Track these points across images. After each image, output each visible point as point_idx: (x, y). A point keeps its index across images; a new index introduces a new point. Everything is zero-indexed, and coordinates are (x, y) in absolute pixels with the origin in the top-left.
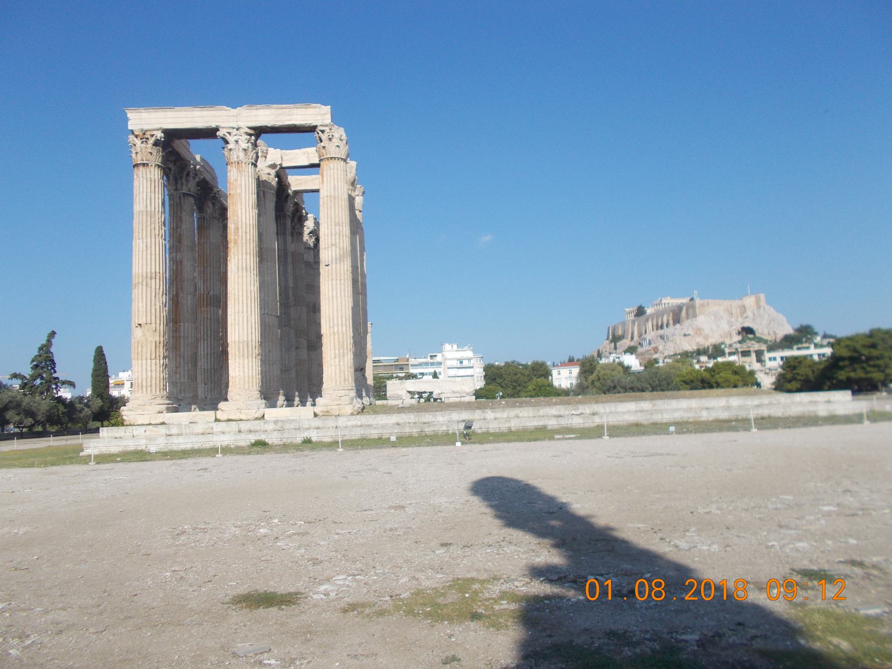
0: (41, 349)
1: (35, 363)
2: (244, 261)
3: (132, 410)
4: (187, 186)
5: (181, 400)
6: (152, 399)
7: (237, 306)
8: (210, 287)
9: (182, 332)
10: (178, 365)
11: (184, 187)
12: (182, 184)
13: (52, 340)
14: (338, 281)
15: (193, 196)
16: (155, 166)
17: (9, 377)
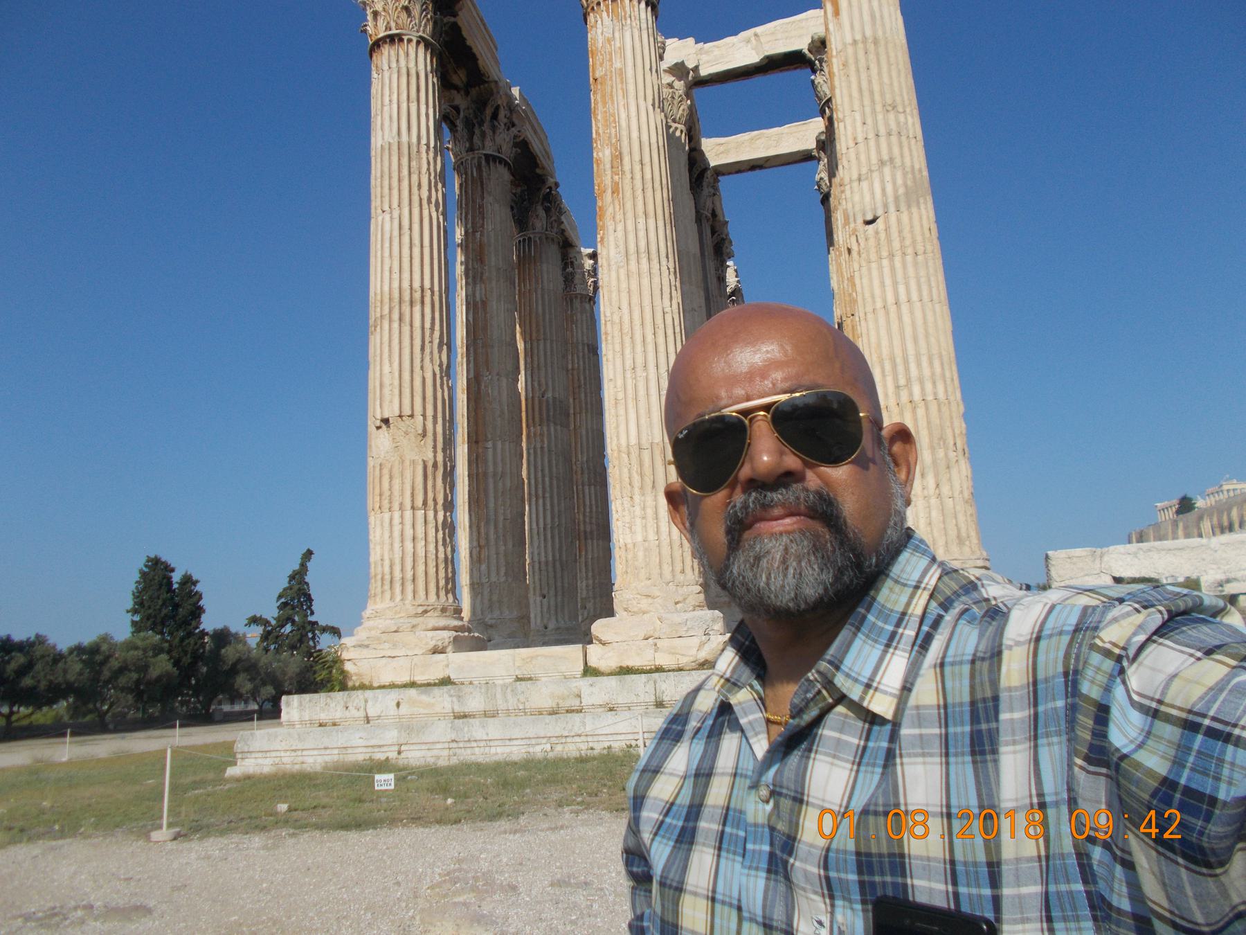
0: (292, 577)
1: (283, 600)
2: (642, 234)
3: (367, 646)
4: (493, 140)
5: (491, 626)
6: (416, 615)
7: (628, 351)
8: (547, 384)
9: (490, 464)
10: (483, 542)
11: (488, 143)
12: (483, 135)
13: (308, 564)
14: (909, 258)
15: (506, 164)
16: (418, 43)
17: (246, 622)
